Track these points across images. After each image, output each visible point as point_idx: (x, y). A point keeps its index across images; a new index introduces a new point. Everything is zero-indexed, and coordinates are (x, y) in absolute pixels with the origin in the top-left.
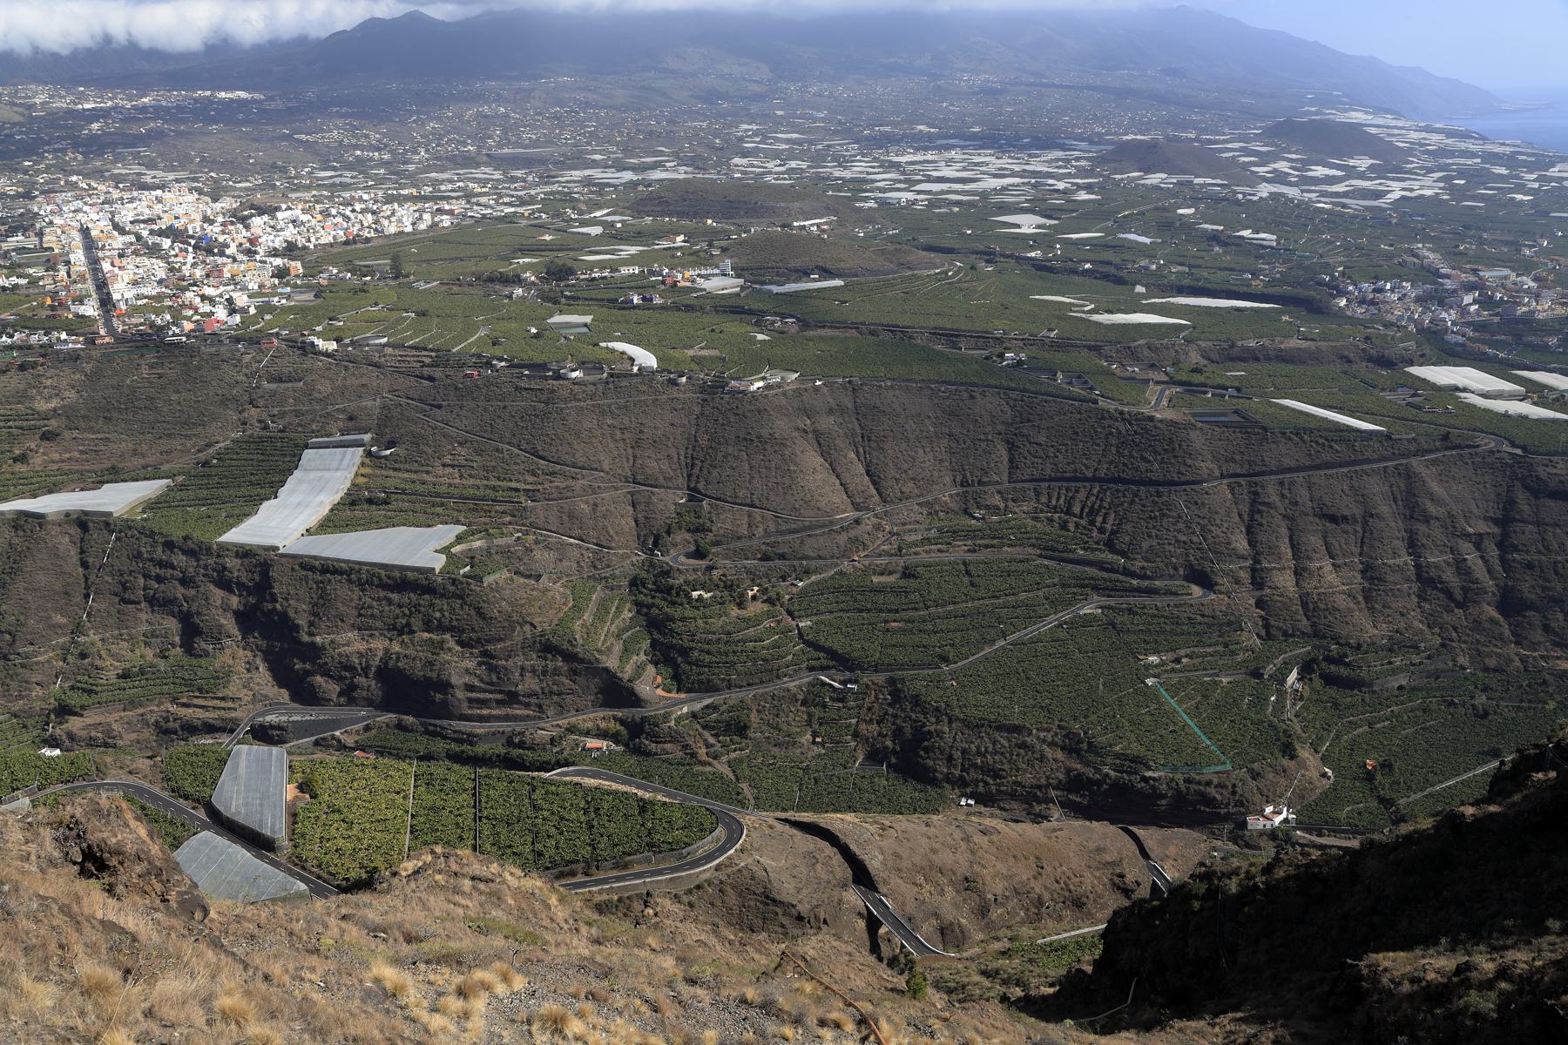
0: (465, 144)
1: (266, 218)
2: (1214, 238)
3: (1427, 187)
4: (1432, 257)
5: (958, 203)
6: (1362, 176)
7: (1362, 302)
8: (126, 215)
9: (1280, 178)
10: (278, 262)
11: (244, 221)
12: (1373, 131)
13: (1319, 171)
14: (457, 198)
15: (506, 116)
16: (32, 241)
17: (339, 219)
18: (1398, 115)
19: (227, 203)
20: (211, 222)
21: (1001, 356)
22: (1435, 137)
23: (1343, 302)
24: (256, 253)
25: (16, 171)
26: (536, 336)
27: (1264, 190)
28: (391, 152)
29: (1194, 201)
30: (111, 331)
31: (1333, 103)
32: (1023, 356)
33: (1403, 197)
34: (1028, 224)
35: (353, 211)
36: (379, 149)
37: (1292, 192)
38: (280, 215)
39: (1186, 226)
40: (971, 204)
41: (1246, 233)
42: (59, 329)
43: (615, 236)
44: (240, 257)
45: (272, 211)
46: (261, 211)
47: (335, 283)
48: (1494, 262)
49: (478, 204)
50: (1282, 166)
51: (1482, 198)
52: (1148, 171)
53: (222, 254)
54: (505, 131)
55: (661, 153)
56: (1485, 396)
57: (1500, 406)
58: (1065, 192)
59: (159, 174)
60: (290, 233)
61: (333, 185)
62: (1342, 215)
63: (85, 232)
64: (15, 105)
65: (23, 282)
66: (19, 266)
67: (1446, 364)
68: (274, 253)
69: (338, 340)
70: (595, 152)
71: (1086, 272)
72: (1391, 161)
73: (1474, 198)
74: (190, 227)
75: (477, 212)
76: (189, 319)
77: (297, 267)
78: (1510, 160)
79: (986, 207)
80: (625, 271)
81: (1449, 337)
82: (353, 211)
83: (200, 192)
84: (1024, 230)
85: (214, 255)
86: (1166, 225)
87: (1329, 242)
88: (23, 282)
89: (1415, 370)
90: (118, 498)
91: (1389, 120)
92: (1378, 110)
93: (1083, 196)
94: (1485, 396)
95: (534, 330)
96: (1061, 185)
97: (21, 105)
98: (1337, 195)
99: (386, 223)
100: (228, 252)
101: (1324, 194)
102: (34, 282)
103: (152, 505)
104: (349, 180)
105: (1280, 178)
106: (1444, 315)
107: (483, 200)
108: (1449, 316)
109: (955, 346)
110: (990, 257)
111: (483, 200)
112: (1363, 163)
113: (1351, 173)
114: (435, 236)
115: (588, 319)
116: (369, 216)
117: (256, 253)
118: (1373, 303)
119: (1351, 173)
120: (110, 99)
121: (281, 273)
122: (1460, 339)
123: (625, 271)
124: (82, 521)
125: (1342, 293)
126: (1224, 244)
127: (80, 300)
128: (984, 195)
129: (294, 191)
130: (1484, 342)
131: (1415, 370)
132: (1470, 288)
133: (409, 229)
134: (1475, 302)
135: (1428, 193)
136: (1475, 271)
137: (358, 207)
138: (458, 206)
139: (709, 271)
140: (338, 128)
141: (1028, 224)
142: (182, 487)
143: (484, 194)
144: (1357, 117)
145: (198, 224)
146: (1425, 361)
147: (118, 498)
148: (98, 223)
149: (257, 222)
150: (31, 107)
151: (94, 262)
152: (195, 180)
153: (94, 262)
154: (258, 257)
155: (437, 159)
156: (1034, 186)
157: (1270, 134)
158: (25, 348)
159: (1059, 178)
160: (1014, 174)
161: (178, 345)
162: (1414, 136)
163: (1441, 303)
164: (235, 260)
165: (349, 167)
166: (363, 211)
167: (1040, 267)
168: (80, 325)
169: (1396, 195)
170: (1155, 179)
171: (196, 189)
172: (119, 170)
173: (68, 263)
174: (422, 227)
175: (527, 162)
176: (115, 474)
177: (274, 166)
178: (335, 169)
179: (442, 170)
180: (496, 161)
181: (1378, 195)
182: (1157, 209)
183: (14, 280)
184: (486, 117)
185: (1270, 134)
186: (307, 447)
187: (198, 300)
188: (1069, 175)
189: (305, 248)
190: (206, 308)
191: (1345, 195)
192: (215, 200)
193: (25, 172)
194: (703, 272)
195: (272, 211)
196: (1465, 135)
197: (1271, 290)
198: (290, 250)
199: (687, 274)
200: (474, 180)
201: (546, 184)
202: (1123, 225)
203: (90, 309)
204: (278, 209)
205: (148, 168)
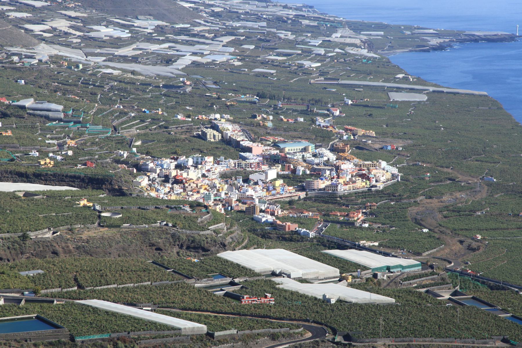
3: (219, 53)
6: (149, 39)
7: (166, 179)
9: (58, 38)
13: (104, 31)
23: (144, 181)
27: (44, 52)
37: (76, 55)
41: (29, 103)
48: (294, 133)
50: (62, 25)
51: (272, 64)
56: (302, 281)
57: (315, 290)
62: (132, 83)
67: (259, 246)
73: (265, 63)
81: (258, 215)
87: (123, 113)
89: (228, 255)
94: (302, 281)
98: (124, 59)
101: (112, 58)
105: (58, 38)
106: (250, 192)
108: (255, 193)
112: (147, 25)
118: (177, 181)
125: (142, 170)
130: (294, 220)
131: (228, 255)
132: (272, 161)
134: (279, 176)
135: (220, 59)
136: (275, 145)
163: (246, 180)
169: (187, 60)
181: (168, 61)
191: (135, 59)
197: (66, 169)
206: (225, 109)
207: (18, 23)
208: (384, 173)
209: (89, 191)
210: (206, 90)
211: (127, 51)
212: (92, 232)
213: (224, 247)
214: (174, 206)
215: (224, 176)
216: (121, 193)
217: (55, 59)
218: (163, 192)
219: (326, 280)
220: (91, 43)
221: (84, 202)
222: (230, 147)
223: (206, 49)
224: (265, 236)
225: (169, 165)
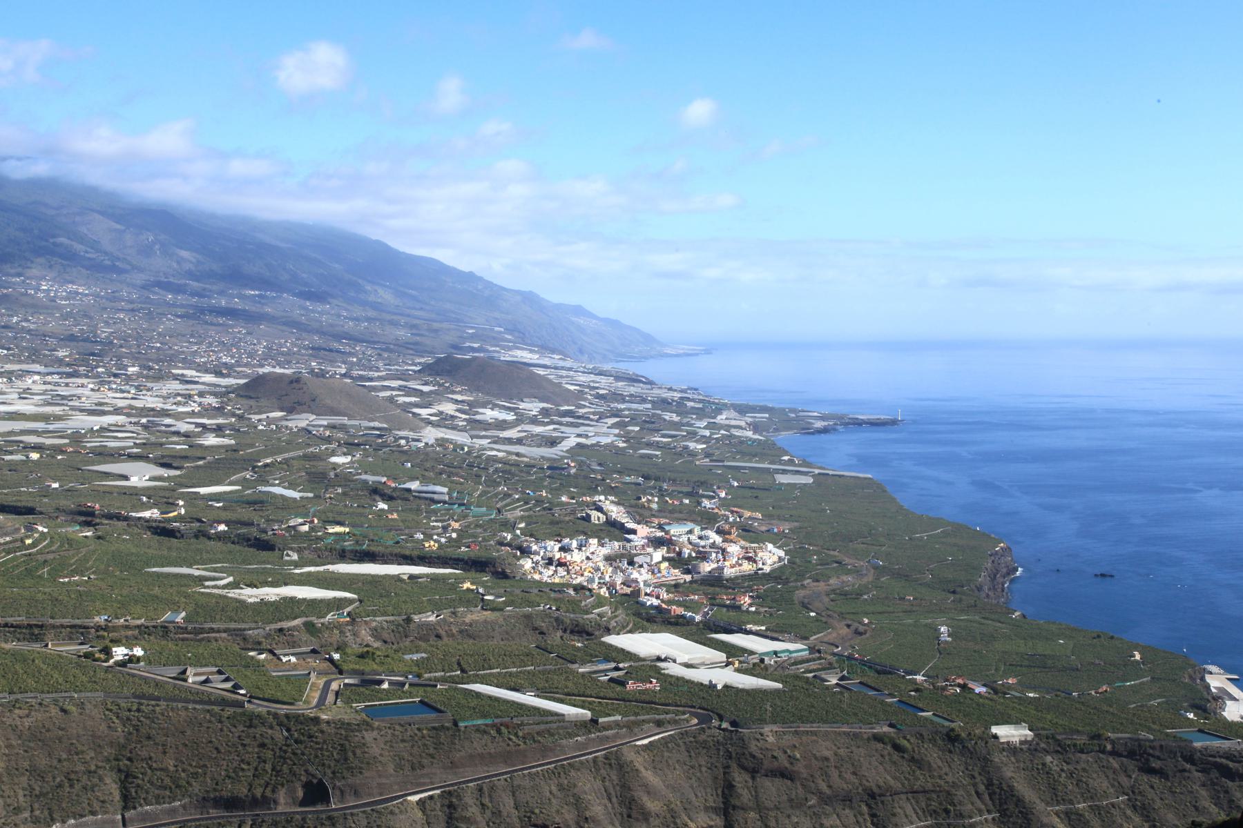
2: (377, 492)
3: (604, 435)
4: (617, 512)
5: (37, 448)
6: (534, 421)
7: (550, 561)
9: (445, 421)
12: (541, 372)
13: (489, 414)
18: (566, 356)
21: (107, 652)
22: (604, 381)
23: (527, 564)
27: (431, 435)
29: (350, 447)
31: (496, 340)
32: (138, 652)
33: (578, 444)
34: (140, 476)
37: (462, 438)
39: (343, 478)
40: (59, 449)
41: (414, 485)
48: (680, 515)
50: (449, 408)
51: (657, 446)
52: (291, 410)
58: (187, 435)
62: (517, 465)
67: (644, 630)
71: (220, 537)
72: (561, 404)
73: (649, 445)
78: (679, 407)
79: (78, 456)
81: (643, 599)
84: (134, 481)
86: (319, 478)
87: (507, 495)
89: (612, 640)
91: (555, 359)
92: (545, 349)
93: (211, 440)
96: (183, 427)
98: (509, 441)
101: (498, 440)
105: (445, 421)
106: (635, 575)
108: (641, 576)
109: (36, 638)
110: (87, 517)
112: (532, 407)
113: (521, 419)
118: (561, 564)
119: (521, 419)
122: (656, 602)
125: (526, 552)
126: (388, 498)
128: (77, 438)
130: (679, 604)
131: (612, 640)
132: (657, 543)
134: (664, 559)
135: (605, 440)
136: (661, 527)
141: (140, 476)
144: (524, 355)
146: (622, 629)
156: (145, 427)
157: (431, 370)
159: (179, 417)
160: (117, 411)
162: (583, 378)
163: (631, 563)
167: (162, 531)
169: (572, 442)
170: (302, 420)
181: (553, 442)
182: (306, 457)
185: (431, 370)
188: (193, 414)
191: (519, 441)
196: (634, 380)
202: (264, 475)
206: (609, 491)
207: (406, 407)
208: (771, 556)
209: (473, 574)
210: (591, 473)
211: (512, 433)
212: (475, 615)
213: (608, 631)
214: (558, 589)
215: (609, 559)
216: (503, 576)
217: (441, 442)
218: (547, 575)
219: (712, 665)
220: (476, 425)
221: (467, 585)
222: (615, 529)
223: (590, 431)
224: (650, 620)
225: (553, 547)
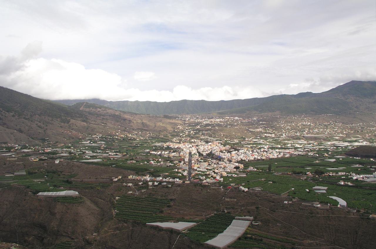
0: (297, 133)
1: (236, 152)
8: (201, 148)
10: (237, 164)
11: (229, 152)
14: (292, 149)
15: (310, 125)
16: (177, 155)
17: (257, 153)
19: (228, 147)
20: (221, 151)
24: (232, 161)
25: (178, 136)
26: (308, 192)
28: (276, 135)
30: (189, 180)
35: (261, 151)
36: (271, 134)
38: (240, 151)
42: (177, 178)
43: (338, 163)
44: (228, 162)
45: (238, 150)
46: (236, 150)
47: (251, 171)
49: (298, 151)
53: (223, 161)
54: (309, 129)
55: (358, 137)
59: (212, 138)
60: (242, 157)
61: (257, 143)
63: (190, 153)
64: (181, 120)
65: (172, 165)
66: (173, 161)
68: (238, 162)
69: (248, 188)
70: (336, 136)
74: (216, 153)
75: (297, 153)
76: (209, 178)
77: (241, 166)
80: (340, 174)
82: (261, 151)
83: (221, 144)
85: (221, 161)
88: (172, 165)
90: (180, 226)
95: (307, 190)
97: (183, 120)
99: (270, 155)
100: (225, 161)
102: (175, 164)
103: (191, 229)
104: (261, 142)
107: (299, 149)
111: (299, 149)
114: (283, 159)
115: (326, 188)
116: (265, 153)
117: (232, 161)
120: (204, 119)
121: (237, 168)
123: (340, 174)
124: (171, 231)
127: (184, 171)
129: (246, 145)
133: (276, 157)
137: (262, 150)
138: (292, 151)
139: (370, 176)
140: (261, 128)
142: (198, 226)
143: (301, 148)
145: (218, 152)
147: (180, 226)
148: (194, 151)
149: (234, 153)
150: (185, 121)
151: (190, 161)
152: (221, 140)
153: (190, 161)
154: (232, 163)
155: (288, 137)
158: (168, 182)
161: (205, 186)
164: (226, 163)
165: (262, 138)
166: (264, 151)
168: (183, 177)
171: (220, 143)
172: (203, 137)
173: (184, 160)
174: (280, 156)
175: (315, 139)
176: (183, 220)
177: (242, 137)
178: (259, 139)
179: (289, 140)
180: (307, 139)
183: (170, 164)
184: (304, 125)
186: (234, 219)
187: (213, 173)
189: (245, 160)
190: (215, 175)
192: (224, 146)
193: (180, 137)
194: (367, 176)
195: (238, 150)
198: (241, 162)
199: (361, 176)
200: (298, 144)
201: (320, 145)
203: (185, 173)
204: (240, 150)
205: (210, 137)
